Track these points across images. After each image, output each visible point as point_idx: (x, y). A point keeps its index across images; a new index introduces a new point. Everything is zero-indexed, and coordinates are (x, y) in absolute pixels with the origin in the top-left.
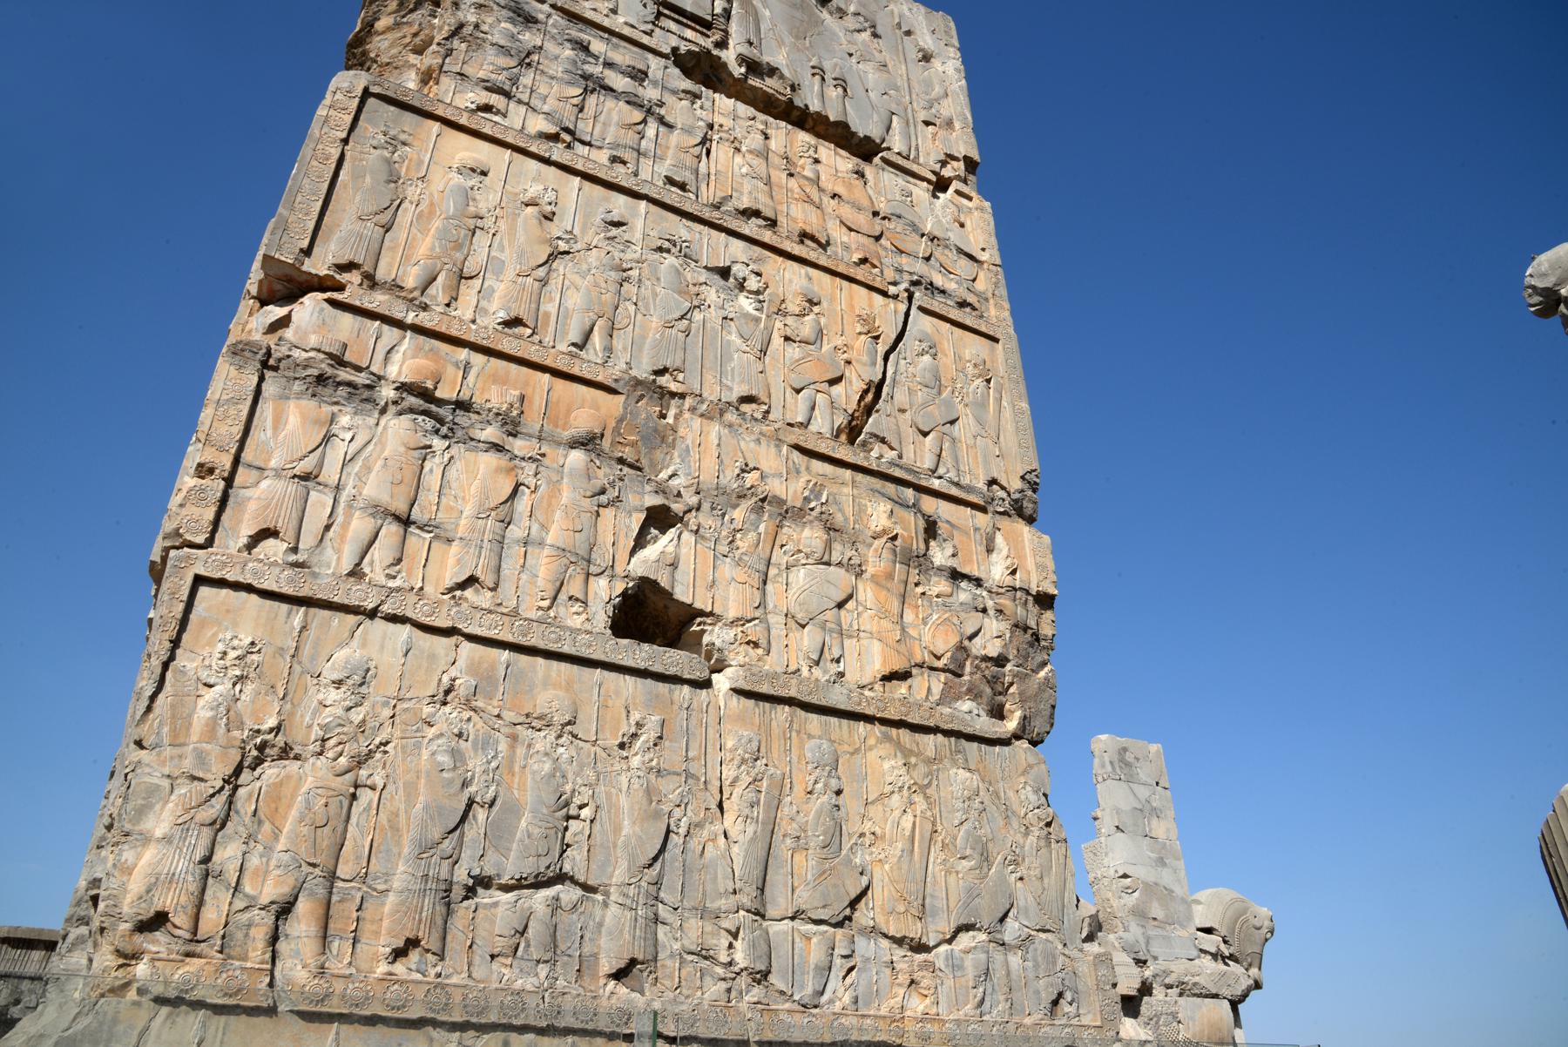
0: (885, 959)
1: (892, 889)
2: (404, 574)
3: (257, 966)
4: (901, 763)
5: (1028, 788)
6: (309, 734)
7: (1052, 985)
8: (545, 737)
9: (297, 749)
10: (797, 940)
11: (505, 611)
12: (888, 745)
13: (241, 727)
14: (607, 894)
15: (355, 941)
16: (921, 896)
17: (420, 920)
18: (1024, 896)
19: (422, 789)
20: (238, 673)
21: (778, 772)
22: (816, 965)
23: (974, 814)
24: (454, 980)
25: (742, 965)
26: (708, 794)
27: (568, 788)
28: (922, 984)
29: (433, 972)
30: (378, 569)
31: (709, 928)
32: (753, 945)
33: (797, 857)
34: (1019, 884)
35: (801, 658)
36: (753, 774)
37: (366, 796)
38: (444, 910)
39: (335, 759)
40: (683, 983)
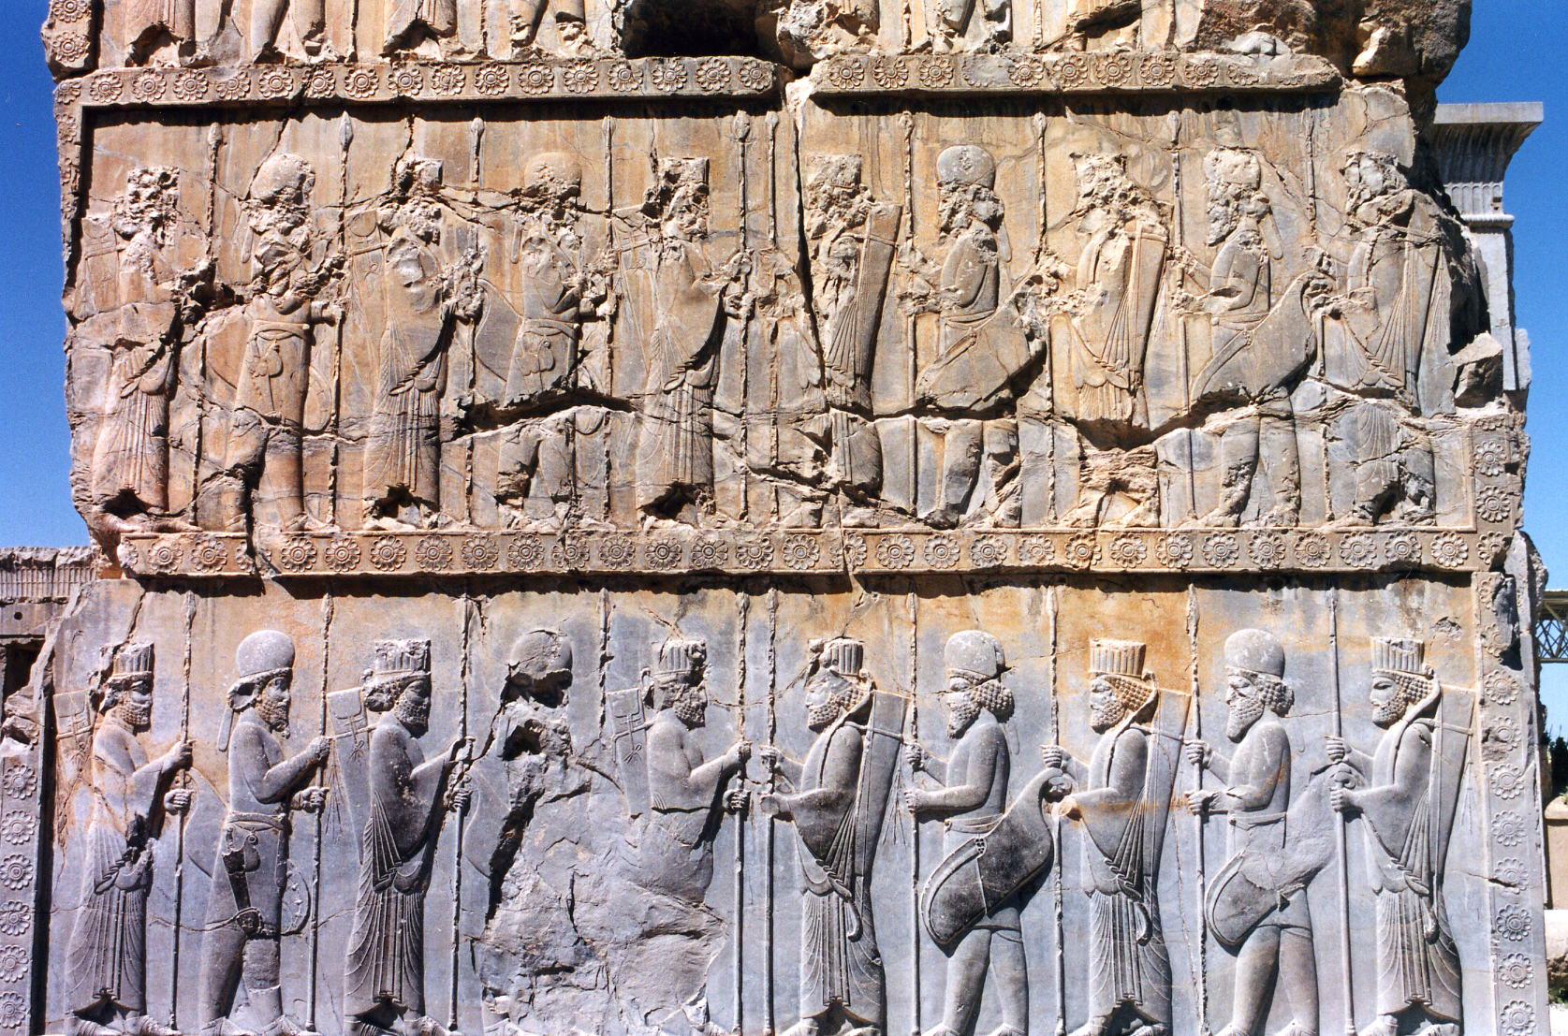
0: (1069, 454)
1: (1084, 353)
2: (329, 42)
3: (232, 535)
4: (1108, 156)
5: (1366, 163)
6: (247, 271)
7: (1378, 473)
8: (540, 218)
9: (238, 291)
10: (922, 436)
11: (466, 58)
12: (1086, 133)
13: (170, 276)
14: (640, 408)
15: (335, 498)
16: (1135, 359)
17: (403, 466)
18: (1338, 339)
19: (389, 312)
20: (155, 214)
21: (891, 207)
22: (951, 471)
23: (1245, 222)
24: (454, 529)
25: (836, 480)
26: (780, 255)
27: (575, 281)
28: (1131, 486)
29: (427, 522)
30: (296, 44)
31: (786, 435)
32: (850, 451)
33: (922, 324)
34: (1330, 322)
35: (933, 23)
36: (848, 216)
37: (326, 335)
38: (431, 451)
39: (280, 295)
40: (752, 508)
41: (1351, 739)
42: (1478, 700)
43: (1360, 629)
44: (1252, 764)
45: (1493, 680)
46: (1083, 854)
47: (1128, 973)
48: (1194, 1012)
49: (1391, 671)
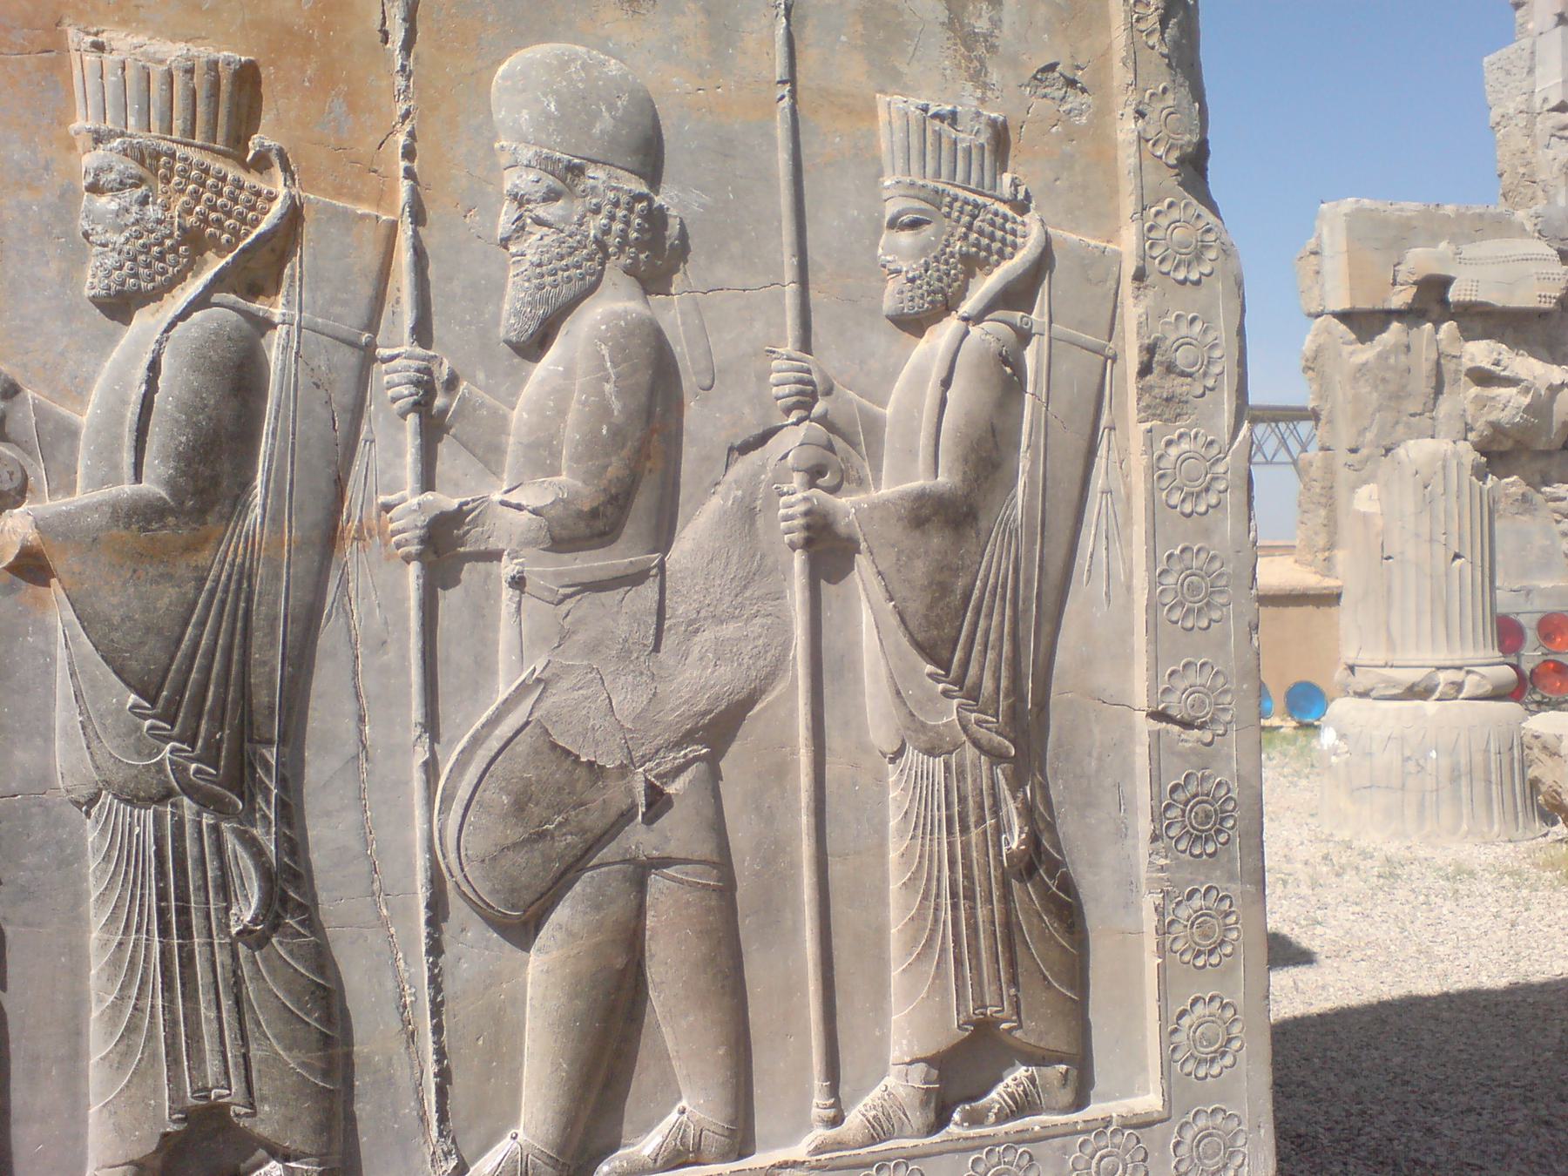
41: (829, 360)
42: (1129, 268)
43: (852, 72)
44: (571, 417)
45: (1163, 221)
46: (63, 686)
47: (207, 1030)
48: (409, 1110)
49: (931, 184)
